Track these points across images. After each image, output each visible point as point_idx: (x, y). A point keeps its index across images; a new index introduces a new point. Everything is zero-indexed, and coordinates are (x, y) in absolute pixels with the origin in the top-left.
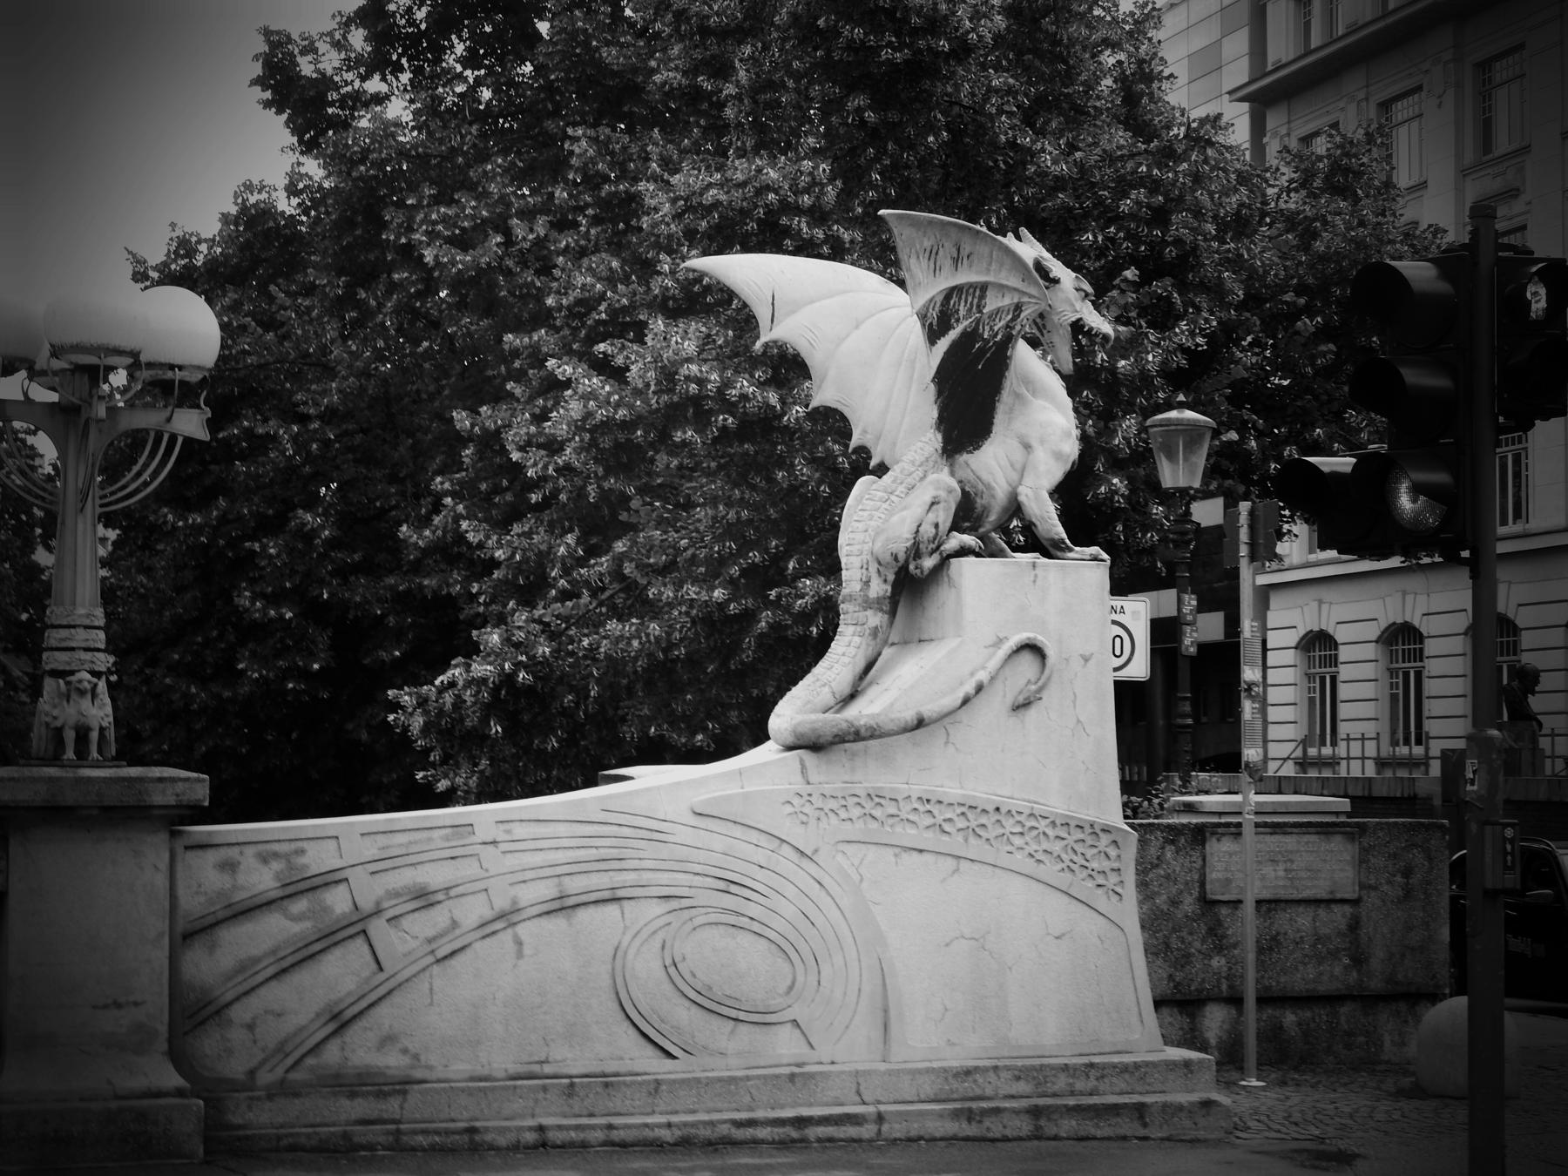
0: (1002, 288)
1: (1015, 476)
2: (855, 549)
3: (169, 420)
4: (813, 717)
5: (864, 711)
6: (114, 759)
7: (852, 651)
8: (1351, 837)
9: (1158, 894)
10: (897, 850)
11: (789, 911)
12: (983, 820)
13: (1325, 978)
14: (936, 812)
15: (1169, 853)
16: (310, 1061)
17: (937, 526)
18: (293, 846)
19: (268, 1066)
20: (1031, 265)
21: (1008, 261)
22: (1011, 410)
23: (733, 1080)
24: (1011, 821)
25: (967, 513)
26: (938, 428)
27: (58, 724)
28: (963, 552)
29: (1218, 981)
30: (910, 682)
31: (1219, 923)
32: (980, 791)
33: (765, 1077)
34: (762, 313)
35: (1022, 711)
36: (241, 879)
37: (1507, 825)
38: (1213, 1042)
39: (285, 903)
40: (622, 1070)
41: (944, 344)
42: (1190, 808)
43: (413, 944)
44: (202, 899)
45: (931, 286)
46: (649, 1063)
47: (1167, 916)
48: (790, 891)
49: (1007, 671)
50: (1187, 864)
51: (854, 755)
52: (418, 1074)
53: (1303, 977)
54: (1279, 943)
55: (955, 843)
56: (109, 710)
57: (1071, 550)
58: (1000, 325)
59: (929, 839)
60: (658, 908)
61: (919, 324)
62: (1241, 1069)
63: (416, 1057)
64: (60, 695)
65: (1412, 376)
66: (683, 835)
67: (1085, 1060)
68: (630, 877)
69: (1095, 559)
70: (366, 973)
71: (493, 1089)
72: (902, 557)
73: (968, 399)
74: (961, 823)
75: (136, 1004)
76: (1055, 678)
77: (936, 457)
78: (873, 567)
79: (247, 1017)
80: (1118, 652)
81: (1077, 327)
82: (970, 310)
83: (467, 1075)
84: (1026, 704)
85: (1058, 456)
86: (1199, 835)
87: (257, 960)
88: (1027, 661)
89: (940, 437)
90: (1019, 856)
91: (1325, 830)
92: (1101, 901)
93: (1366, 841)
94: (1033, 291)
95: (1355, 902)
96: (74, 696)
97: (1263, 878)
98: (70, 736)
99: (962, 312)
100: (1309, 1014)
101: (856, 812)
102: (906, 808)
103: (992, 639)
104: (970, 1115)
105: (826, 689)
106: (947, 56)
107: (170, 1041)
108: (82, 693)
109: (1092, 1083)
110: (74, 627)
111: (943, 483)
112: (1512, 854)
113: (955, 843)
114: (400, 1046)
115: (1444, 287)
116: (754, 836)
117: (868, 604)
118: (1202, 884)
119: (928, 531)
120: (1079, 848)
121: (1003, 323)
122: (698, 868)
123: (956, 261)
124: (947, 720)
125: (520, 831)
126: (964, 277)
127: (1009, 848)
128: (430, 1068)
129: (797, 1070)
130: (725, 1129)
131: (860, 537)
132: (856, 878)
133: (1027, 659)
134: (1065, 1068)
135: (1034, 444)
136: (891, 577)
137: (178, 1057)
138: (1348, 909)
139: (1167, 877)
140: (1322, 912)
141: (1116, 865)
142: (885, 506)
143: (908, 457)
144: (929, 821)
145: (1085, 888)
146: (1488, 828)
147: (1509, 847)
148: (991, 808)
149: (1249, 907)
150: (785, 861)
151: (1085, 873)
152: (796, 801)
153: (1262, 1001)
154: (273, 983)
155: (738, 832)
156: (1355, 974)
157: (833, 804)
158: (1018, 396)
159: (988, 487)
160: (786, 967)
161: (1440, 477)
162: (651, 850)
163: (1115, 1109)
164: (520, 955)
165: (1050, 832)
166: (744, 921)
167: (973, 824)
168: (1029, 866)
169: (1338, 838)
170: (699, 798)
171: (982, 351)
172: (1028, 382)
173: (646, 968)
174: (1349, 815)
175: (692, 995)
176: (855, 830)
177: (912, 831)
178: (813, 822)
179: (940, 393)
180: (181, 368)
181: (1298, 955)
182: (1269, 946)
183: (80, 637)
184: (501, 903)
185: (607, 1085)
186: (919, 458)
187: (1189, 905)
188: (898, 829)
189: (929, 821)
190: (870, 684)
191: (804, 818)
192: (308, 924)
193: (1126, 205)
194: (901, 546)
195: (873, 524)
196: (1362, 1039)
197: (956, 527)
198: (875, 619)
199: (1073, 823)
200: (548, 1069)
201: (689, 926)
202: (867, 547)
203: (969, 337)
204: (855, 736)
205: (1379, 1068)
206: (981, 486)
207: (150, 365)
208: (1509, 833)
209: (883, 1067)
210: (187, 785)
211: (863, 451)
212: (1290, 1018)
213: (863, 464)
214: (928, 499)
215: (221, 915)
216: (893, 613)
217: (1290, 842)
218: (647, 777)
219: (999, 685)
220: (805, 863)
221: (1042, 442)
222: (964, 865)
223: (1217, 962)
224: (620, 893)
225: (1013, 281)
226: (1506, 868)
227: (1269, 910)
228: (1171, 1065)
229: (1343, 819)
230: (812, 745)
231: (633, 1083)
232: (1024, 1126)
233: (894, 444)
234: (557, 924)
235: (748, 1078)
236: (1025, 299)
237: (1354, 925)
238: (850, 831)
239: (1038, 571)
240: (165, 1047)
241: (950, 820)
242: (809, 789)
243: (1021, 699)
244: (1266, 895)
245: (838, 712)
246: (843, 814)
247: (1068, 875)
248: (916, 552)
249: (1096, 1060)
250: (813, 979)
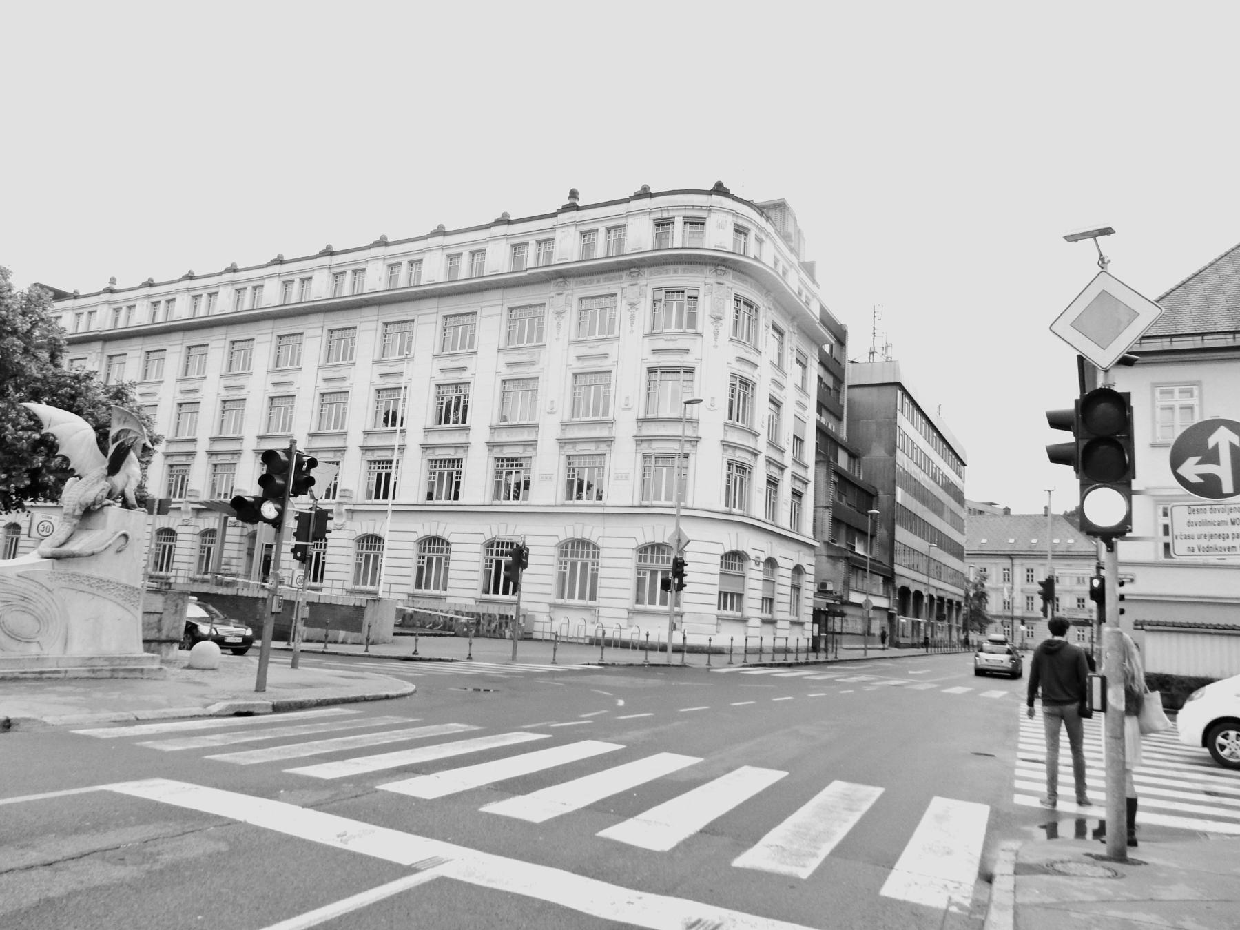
25: (110, 495)
34: (46, 424)
59: (87, 588)
66: (13, 582)
88: (123, 540)
92: (132, 609)
104: (93, 671)
106: (8, 333)
111: (104, 484)
113: (94, 590)
126: (126, 427)
130: (17, 675)
145: (128, 605)
150: (44, 592)
163: (134, 670)
176: (64, 584)
193: (62, 391)
203: (122, 444)
204: (72, 556)
232: (108, 674)
237: (160, 620)
238: (64, 584)
248: (94, 503)
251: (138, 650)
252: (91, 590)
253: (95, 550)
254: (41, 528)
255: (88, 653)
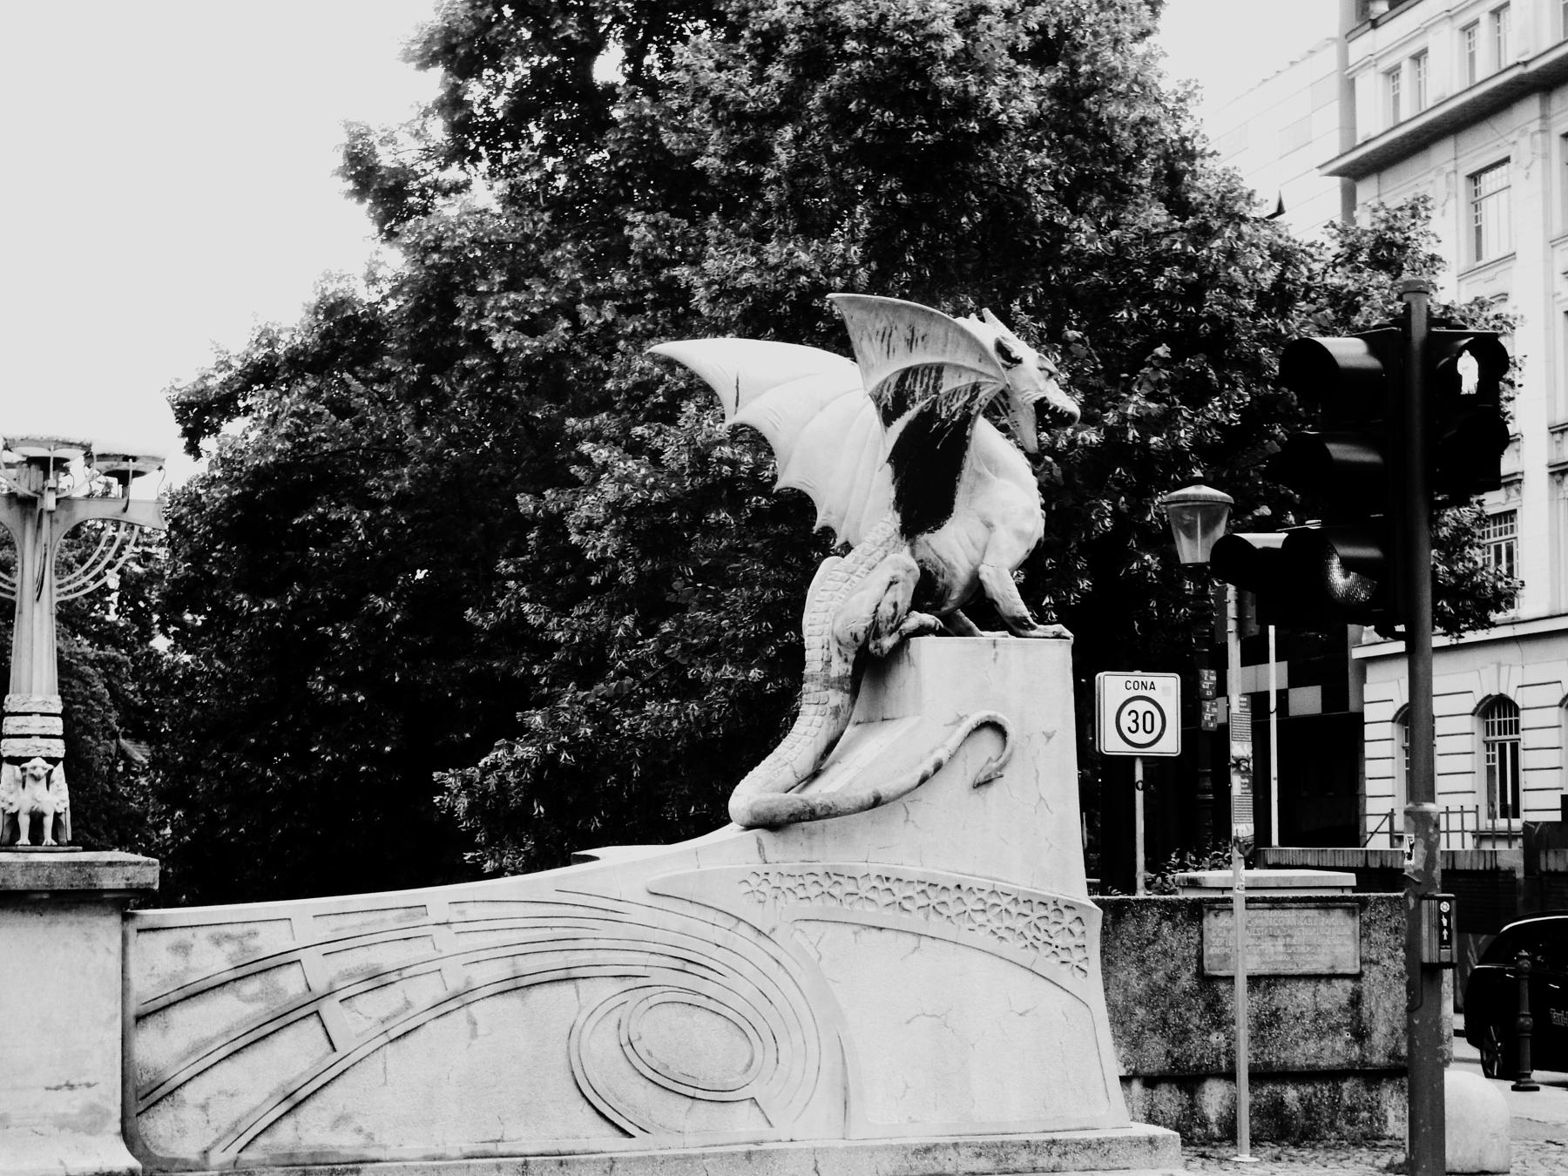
0: (958, 368)
1: (976, 555)
2: (816, 629)
3: (125, 510)
4: (770, 796)
5: (820, 793)
6: (69, 843)
7: (814, 730)
8: (1351, 912)
9: (1156, 970)
10: (856, 928)
11: (747, 990)
12: (944, 897)
13: (1327, 1053)
14: (895, 890)
15: (1166, 928)
16: (262, 1141)
17: (895, 605)
18: (247, 927)
19: (221, 1146)
20: (990, 346)
21: (964, 343)
22: (972, 490)
23: (687, 1158)
24: (973, 898)
25: (928, 591)
26: (897, 509)
27: (13, 810)
28: (923, 631)
29: (1217, 1056)
30: (873, 759)
31: (1218, 999)
32: (942, 869)
33: (722, 1155)
34: (726, 395)
35: (983, 788)
36: (194, 961)
37: (1441, 900)
38: (1213, 1118)
39: (238, 984)
40: (578, 1149)
41: (899, 425)
42: (1194, 884)
43: (367, 1024)
44: (155, 981)
45: (881, 365)
46: (605, 1140)
47: (1164, 992)
48: (747, 969)
49: (967, 748)
50: (1185, 940)
51: (811, 834)
52: (372, 1154)
53: (1304, 1053)
54: (1279, 1019)
55: (915, 921)
56: (65, 794)
57: (1033, 628)
58: (957, 405)
59: (889, 917)
60: (617, 986)
61: (872, 405)
62: (1234, 1144)
63: (370, 1136)
64: (17, 781)
65: (1338, 451)
67: (1048, 1137)
68: (585, 957)
69: (1058, 636)
70: (319, 1054)
71: (448, 1167)
72: (861, 636)
73: (927, 477)
74: (922, 901)
75: (89, 1085)
76: (1017, 754)
77: (896, 537)
78: (834, 647)
79: (201, 1100)
80: (1148, 728)
81: (1041, 406)
82: (926, 391)
83: (421, 1154)
84: (988, 782)
85: (1020, 534)
86: (1196, 912)
87: (212, 1041)
88: (988, 739)
89: (898, 517)
90: (981, 933)
91: (1325, 904)
92: (1066, 976)
93: (1366, 916)
94: (990, 371)
95: (1357, 977)
96: (29, 782)
97: (1262, 954)
98: (24, 822)
99: (918, 392)
100: (1310, 1090)
101: (816, 890)
102: (864, 886)
103: (952, 717)
105: (788, 768)
106: (978, 138)
107: (123, 1121)
108: (37, 779)
109: (1054, 1160)
110: (30, 714)
111: (902, 563)
112: (1448, 928)
113: (915, 921)
114: (353, 1126)
115: (1372, 363)
116: (711, 916)
117: (828, 684)
118: (1200, 959)
119: (886, 610)
120: (1042, 924)
121: (961, 403)
122: (655, 948)
123: (910, 343)
124: (905, 799)
125: (473, 912)
126: (919, 358)
127: (971, 925)
128: (385, 1147)
129: (753, 1148)
131: (821, 617)
132: (815, 957)
133: (988, 736)
134: (1027, 1145)
135: (995, 522)
136: (852, 657)
137: (129, 1137)
138: (1349, 984)
139: (1165, 953)
140: (1322, 987)
141: (1080, 942)
142: (846, 586)
143: (869, 538)
144: (888, 898)
145: (1050, 965)
146: (1425, 903)
147: (1445, 922)
148: (951, 886)
149: (1241, 984)
150: (743, 940)
151: (1050, 949)
152: (754, 880)
153: (1259, 1076)
154: (226, 1064)
155: (694, 910)
156: (1357, 1049)
157: (791, 883)
158: (979, 475)
159: (949, 566)
160: (744, 1044)
161: (1371, 553)
162: (606, 929)
164: (474, 1035)
165: (1012, 908)
166: (701, 1000)
167: (934, 902)
168: (992, 943)
169: (1339, 913)
170: (655, 879)
171: (941, 431)
172: (989, 461)
173: (601, 1052)
174: (1354, 889)
175: (649, 1074)
176: (813, 908)
177: (870, 908)
178: (770, 901)
179: (897, 473)
180: (135, 459)
181: (1299, 1030)
182: (1267, 1023)
183: (35, 725)
184: (455, 984)
185: (561, 1164)
186: (881, 538)
187: (1186, 981)
188: (858, 907)
189: (888, 898)
190: (833, 763)
191: (762, 898)
192: (261, 1006)
193: (1160, 283)
194: (861, 626)
195: (838, 603)
196: (1365, 1114)
197: (917, 604)
198: (837, 698)
199: (1036, 901)
200: (503, 1148)
201: (646, 1005)
202: (827, 627)
203: (926, 417)
205: (1383, 1143)
206: (941, 566)
207: (103, 457)
208: (1445, 907)
209: (842, 1144)
210: (137, 868)
211: (828, 532)
212: (1291, 1095)
213: (825, 543)
214: (887, 580)
215: (174, 997)
216: (854, 693)
217: (1289, 917)
218: (610, 855)
219: (958, 762)
220: (763, 941)
221: (1004, 521)
222: (925, 942)
223: (1216, 1038)
224: (574, 973)
225: (970, 361)
226: (1441, 942)
227: (1269, 986)
228: (1136, 1143)
229: (1349, 893)
230: (770, 824)
231: (587, 1161)
233: (858, 524)
234: (512, 1001)
235: (704, 1156)
236: (983, 379)
237: (1356, 1000)
238: (808, 910)
239: (998, 649)
240: (118, 1127)
241: (910, 898)
242: (766, 868)
243: (981, 778)
244: (1265, 970)
245: (799, 791)
246: (801, 893)
247: (1031, 951)
248: (874, 631)
249: (1057, 1136)
250: (772, 1056)
251: (1112, 1112)
252: (905, 921)
253: (886, 789)
254: (1127, 721)
255: (932, 1126)
